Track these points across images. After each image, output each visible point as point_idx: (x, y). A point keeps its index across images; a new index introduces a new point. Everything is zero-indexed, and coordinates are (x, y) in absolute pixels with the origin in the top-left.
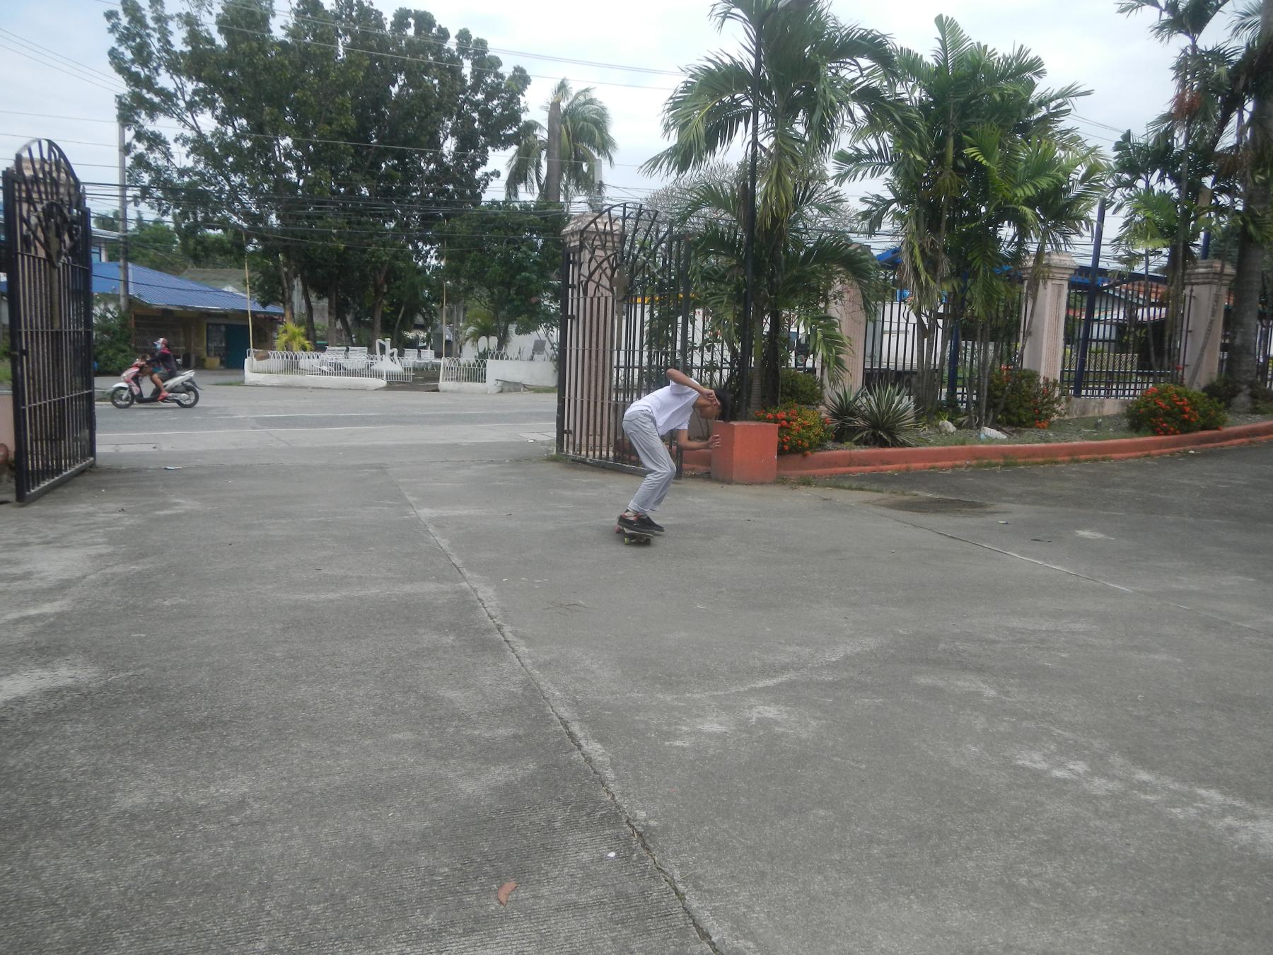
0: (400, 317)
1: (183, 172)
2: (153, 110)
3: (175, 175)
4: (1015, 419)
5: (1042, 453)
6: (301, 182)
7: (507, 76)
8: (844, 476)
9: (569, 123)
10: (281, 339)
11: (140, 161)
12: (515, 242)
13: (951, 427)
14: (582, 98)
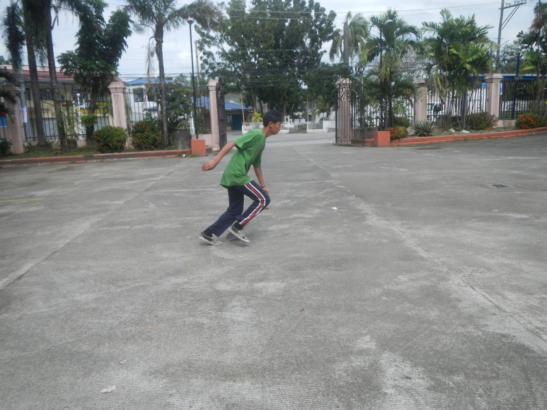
0: (293, 107)
1: (219, 64)
2: (209, 43)
3: (216, 65)
4: (479, 127)
5: (478, 136)
6: (256, 62)
7: (328, 14)
8: (411, 144)
9: (352, 28)
10: (253, 118)
11: (206, 62)
12: (331, 79)
13: (453, 130)
14: (357, 18)
